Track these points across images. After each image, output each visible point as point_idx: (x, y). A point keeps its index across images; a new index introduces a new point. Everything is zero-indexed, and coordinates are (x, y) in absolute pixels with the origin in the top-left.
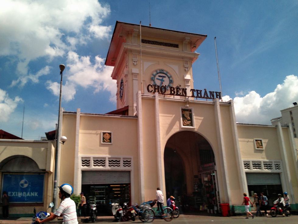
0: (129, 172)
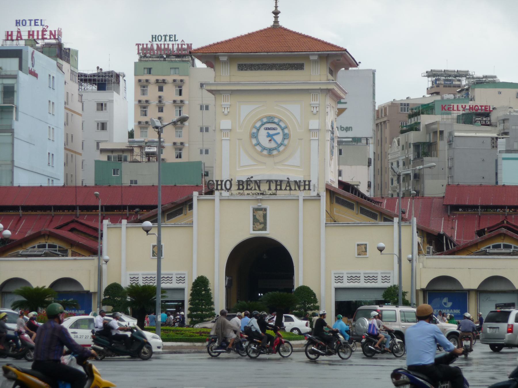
0: (183, 290)
